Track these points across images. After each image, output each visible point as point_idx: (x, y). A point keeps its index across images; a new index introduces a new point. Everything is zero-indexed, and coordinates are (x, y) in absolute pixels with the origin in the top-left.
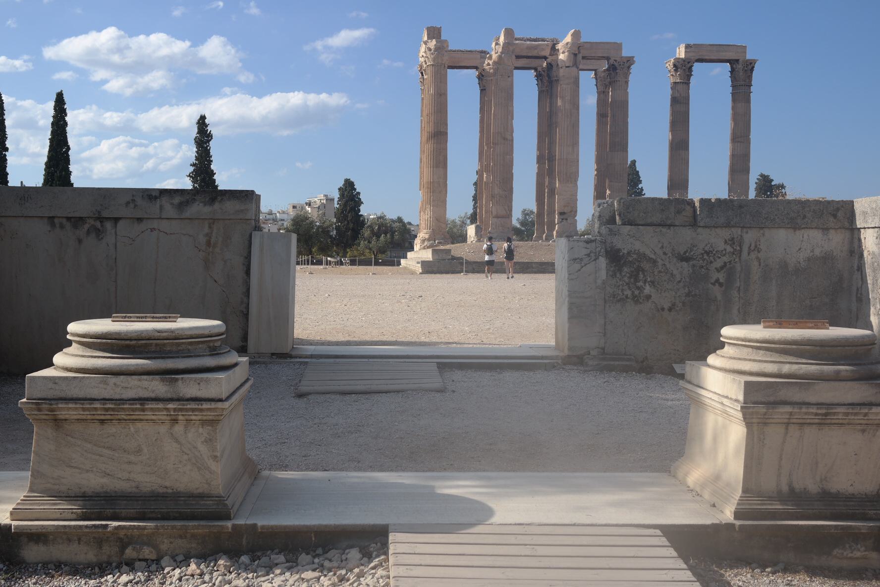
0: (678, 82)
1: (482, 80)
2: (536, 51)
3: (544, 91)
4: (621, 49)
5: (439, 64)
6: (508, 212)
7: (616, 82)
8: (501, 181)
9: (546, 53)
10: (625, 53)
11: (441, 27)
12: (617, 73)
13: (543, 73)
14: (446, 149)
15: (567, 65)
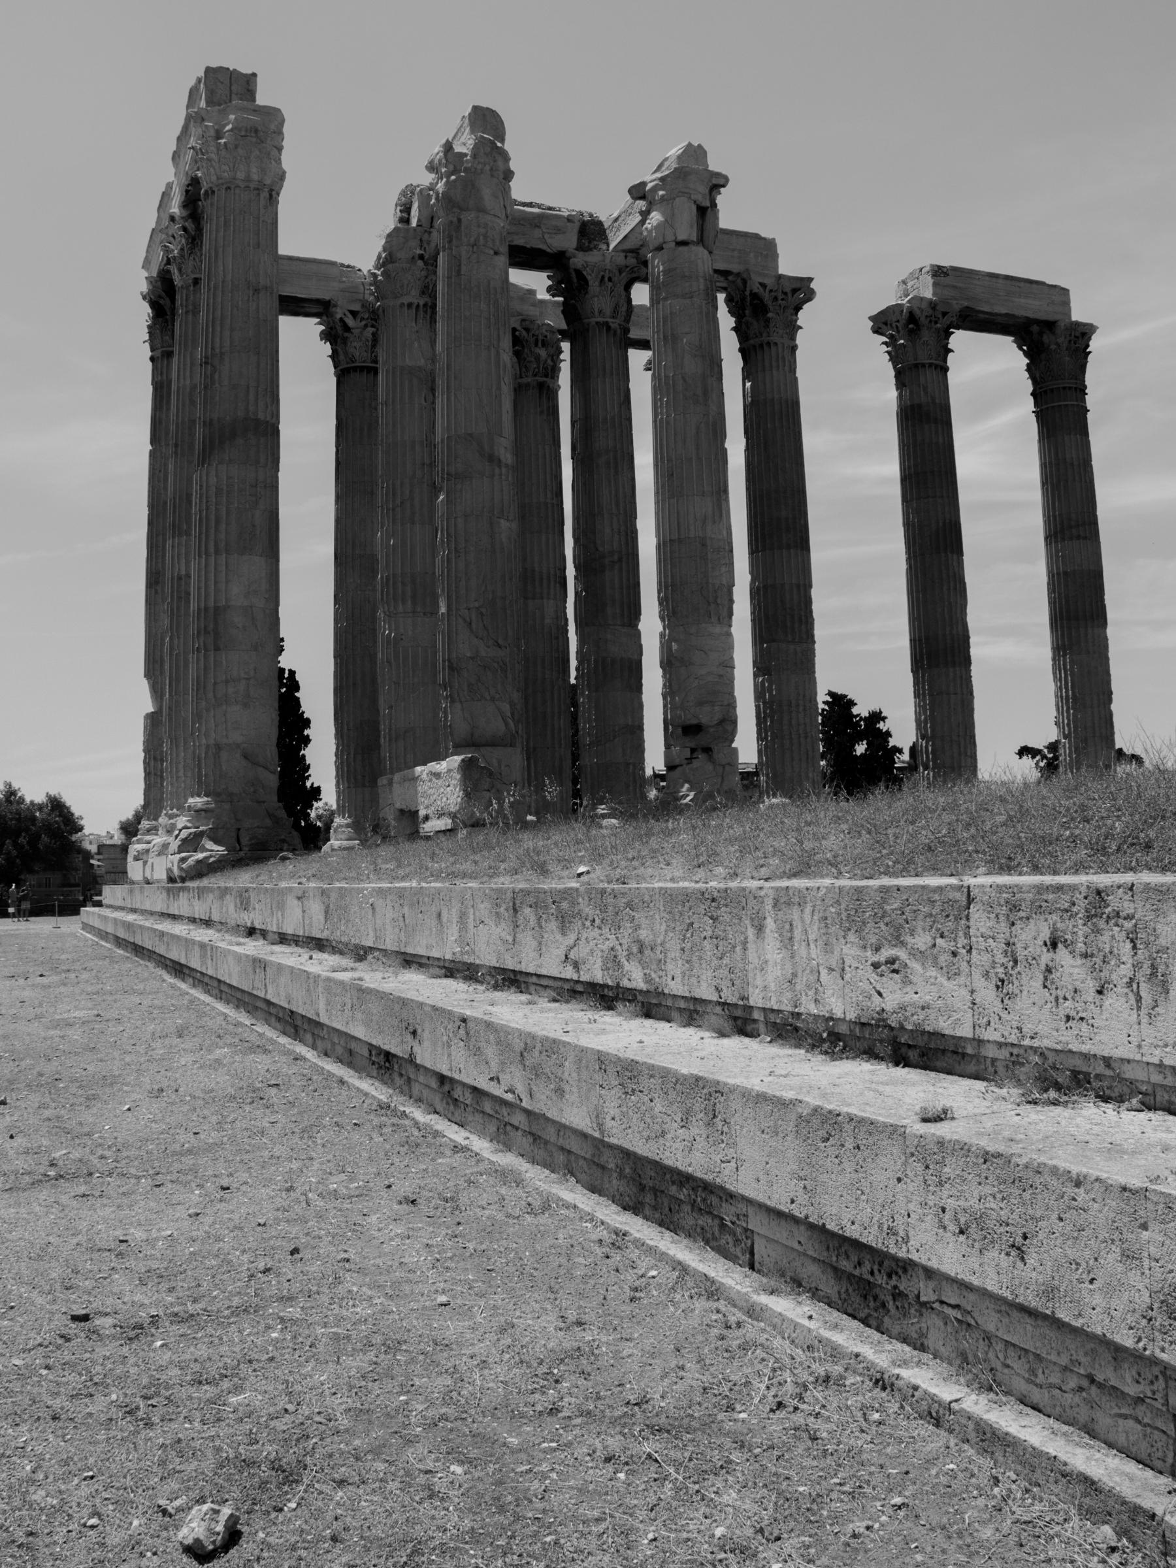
0: (923, 365)
1: (345, 341)
2: (537, 233)
3: (528, 385)
4: (775, 256)
5: (252, 186)
6: (512, 724)
7: (765, 347)
8: (483, 610)
9: (567, 241)
10: (788, 266)
11: (254, 75)
12: (768, 321)
13: (524, 333)
14: (272, 487)
15: (681, 238)
